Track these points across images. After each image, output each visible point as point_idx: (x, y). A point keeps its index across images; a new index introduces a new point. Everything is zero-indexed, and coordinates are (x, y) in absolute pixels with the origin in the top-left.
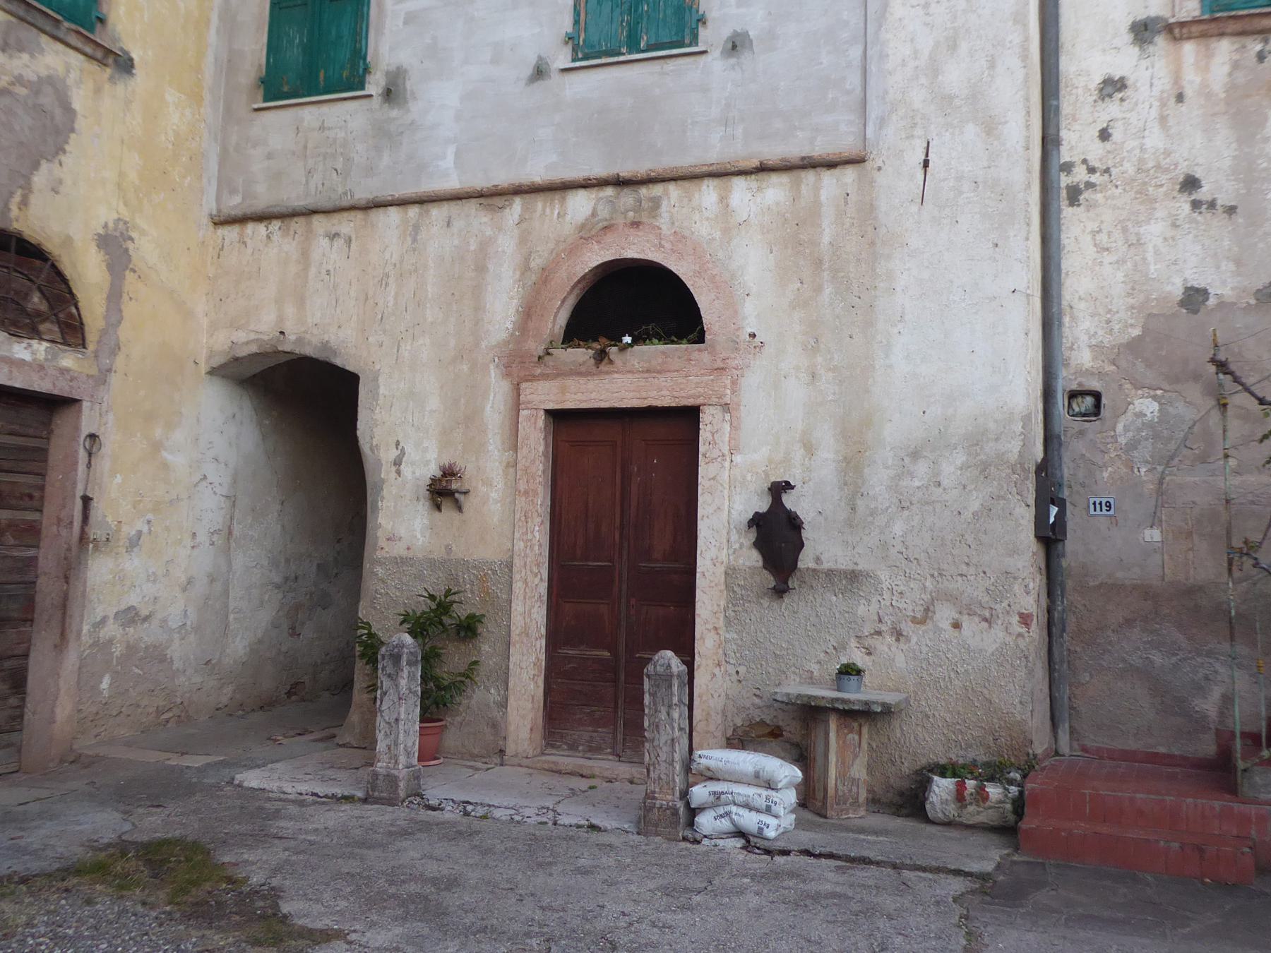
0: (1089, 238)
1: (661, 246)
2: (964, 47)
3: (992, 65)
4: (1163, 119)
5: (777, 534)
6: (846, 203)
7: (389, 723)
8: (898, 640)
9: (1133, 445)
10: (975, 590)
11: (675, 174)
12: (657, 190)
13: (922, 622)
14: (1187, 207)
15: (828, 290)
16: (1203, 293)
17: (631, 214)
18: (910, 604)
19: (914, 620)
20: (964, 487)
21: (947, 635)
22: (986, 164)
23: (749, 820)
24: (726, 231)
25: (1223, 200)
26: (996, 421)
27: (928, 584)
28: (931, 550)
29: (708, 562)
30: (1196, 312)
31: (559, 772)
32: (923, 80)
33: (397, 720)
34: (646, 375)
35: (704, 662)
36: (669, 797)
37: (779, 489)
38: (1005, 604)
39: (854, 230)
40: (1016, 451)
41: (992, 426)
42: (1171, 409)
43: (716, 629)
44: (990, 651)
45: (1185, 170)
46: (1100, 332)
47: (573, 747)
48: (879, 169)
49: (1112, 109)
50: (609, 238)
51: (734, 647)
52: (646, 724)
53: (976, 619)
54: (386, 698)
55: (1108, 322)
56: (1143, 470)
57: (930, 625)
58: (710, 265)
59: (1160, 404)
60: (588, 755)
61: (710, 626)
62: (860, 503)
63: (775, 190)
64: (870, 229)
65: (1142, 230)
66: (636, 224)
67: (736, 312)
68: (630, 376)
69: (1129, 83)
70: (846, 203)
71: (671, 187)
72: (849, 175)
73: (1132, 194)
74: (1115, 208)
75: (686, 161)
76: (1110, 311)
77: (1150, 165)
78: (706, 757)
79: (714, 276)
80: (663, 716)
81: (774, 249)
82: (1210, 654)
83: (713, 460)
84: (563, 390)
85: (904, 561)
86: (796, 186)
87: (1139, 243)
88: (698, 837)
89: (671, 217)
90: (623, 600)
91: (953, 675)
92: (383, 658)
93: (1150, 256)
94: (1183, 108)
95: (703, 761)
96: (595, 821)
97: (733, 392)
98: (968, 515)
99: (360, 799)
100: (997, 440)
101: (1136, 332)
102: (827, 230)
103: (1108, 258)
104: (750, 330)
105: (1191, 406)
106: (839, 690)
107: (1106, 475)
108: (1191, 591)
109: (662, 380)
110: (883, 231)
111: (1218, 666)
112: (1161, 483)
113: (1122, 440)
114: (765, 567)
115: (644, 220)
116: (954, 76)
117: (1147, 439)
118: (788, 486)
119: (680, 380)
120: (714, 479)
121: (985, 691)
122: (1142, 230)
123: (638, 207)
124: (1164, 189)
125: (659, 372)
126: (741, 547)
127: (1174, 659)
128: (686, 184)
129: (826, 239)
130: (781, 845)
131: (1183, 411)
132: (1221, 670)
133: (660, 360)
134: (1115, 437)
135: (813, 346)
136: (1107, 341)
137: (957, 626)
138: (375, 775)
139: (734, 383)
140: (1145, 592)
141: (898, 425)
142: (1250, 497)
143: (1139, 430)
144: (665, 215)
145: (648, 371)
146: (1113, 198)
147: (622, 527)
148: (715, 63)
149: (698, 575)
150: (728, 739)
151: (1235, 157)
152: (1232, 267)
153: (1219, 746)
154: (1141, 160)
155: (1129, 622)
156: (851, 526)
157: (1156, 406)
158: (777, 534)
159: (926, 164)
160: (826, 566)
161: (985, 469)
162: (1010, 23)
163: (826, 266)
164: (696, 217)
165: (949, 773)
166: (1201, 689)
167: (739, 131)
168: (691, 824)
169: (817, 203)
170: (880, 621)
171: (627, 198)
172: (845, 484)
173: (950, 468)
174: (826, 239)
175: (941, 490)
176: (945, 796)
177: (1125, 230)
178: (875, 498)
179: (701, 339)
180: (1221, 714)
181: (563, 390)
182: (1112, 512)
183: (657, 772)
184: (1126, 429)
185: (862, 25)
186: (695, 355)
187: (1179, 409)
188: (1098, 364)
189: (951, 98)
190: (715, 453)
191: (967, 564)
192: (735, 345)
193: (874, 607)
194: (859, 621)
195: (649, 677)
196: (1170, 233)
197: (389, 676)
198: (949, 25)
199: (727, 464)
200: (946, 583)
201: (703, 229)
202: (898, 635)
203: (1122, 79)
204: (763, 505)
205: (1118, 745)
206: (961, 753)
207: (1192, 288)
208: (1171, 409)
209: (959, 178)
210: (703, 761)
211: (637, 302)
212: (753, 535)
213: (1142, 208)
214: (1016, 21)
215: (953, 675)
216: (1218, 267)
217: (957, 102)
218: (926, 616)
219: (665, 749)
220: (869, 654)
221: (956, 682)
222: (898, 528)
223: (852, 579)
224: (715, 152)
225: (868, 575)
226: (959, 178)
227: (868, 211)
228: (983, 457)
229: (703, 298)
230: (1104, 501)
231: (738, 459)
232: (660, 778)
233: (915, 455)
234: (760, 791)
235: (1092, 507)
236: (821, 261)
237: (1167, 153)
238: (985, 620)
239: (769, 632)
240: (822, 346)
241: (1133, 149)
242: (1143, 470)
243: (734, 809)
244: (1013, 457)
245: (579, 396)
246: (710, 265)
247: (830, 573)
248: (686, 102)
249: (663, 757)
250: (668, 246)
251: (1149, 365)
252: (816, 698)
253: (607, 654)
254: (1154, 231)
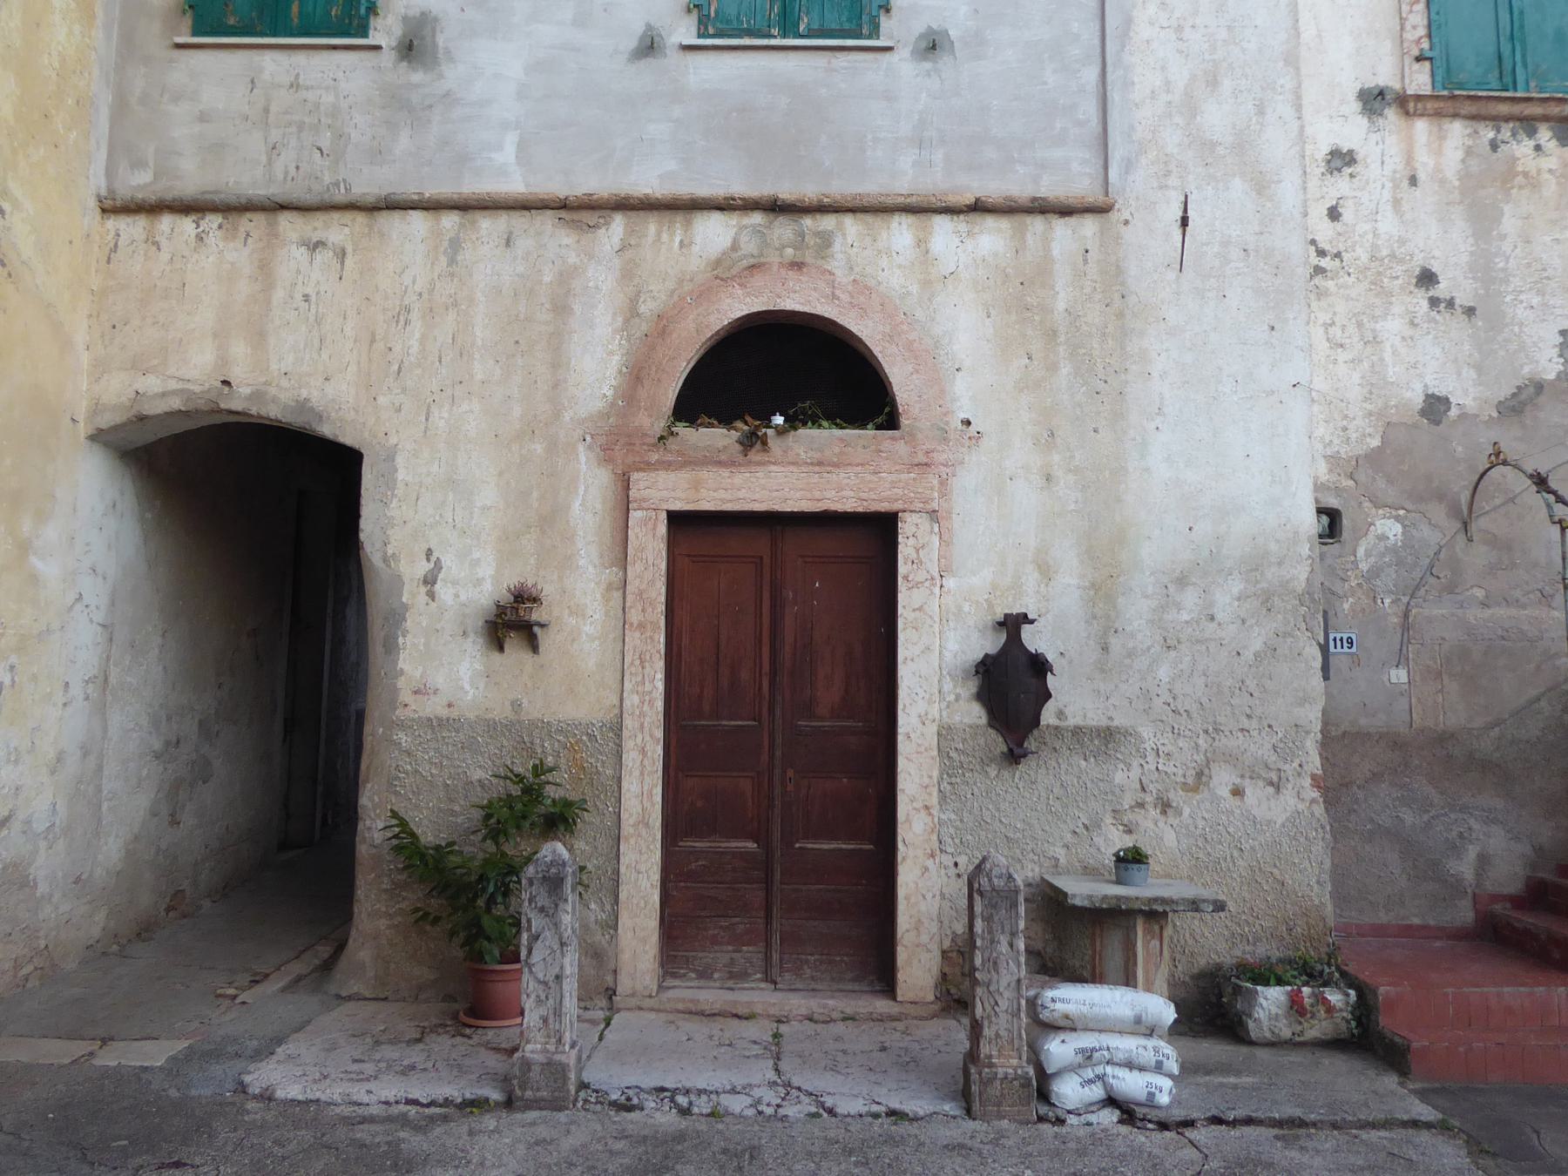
0: (1321, 330)
1: (834, 296)
2: (1227, 84)
3: (1261, 111)
4: (1396, 203)
5: (1011, 684)
6: (1086, 261)
7: (545, 983)
8: (1164, 812)
9: (1375, 572)
10: (1260, 748)
11: (857, 203)
12: (828, 222)
13: (1195, 789)
14: (1425, 304)
15: (1065, 369)
16: (1445, 401)
17: (790, 251)
18: (1179, 767)
19: (1185, 787)
20: (1244, 621)
21: (1226, 806)
22: (1257, 229)
23: (1131, 1084)
24: (926, 283)
25: (1462, 299)
26: (1278, 541)
27: (1201, 742)
28: (1204, 700)
29: (915, 721)
30: (1438, 423)
31: (702, 1014)
32: (1178, 119)
33: (558, 978)
34: (817, 469)
35: (911, 853)
36: (1015, 1062)
37: (1013, 624)
38: (1295, 765)
39: (1098, 297)
40: (1304, 576)
41: (1273, 547)
42: (1414, 532)
43: (927, 807)
44: (1279, 822)
45: (1421, 262)
46: (1336, 441)
47: (705, 974)
48: (1126, 222)
49: (1340, 186)
50: (758, 280)
51: (952, 831)
52: (978, 961)
53: (1261, 783)
54: (538, 945)
55: (1345, 429)
56: (1387, 601)
57: (1204, 794)
58: (905, 327)
59: (1404, 527)
60: (730, 984)
61: (918, 805)
62: (1115, 642)
63: (992, 236)
64: (1117, 296)
65: (1378, 326)
66: (797, 266)
67: (943, 391)
68: (792, 468)
69: (1359, 157)
70: (1086, 261)
71: (848, 220)
72: (1088, 226)
73: (1365, 285)
74: (1348, 298)
75: (869, 188)
76: (1346, 417)
77: (1385, 252)
78: (1063, 1001)
79: (912, 342)
80: (1004, 948)
81: (993, 312)
82: (1464, 809)
83: (918, 585)
84: (696, 485)
85: (1171, 714)
86: (1020, 234)
87: (1375, 341)
88: (1060, 1113)
89: (849, 260)
90: (777, 771)
91: (1236, 854)
92: (531, 882)
93: (1388, 356)
94: (1418, 192)
95: (1058, 1006)
96: (895, 1105)
97: (943, 495)
98: (1248, 655)
99: (497, 1104)
100: (1280, 564)
101: (1375, 442)
102: (1062, 295)
103: (1342, 356)
104: (963, 416)
105: (1435, 530)
106: (1119, 882)
107: (1346, 606)
108: (1443, 739)
109: (839, 477)
110: (1132, 300)
111: (1472, 822)
112: (1406, 615)
113: (1364, 566)
114: (991, 725)
115: (809, 260)
116: (1217, 118)
117: (1390, 566)
118: (1024, 619)
119: (869, 477)
120: (920, 609)
121: (1276, 871)
122: (1378, 326)
123: (800, 241)
124: (1400, 281)
125: (836, 465)
126: (957, 700)
127: (1426, 817)
128: (869, 218)
129: (1061, 305)
130: (1178, 1114)
131: (1429, 536)
132: (1476, 826)
133: (837, 450)
134: (1355, 563)
135: (1049, 439)
136: (1344, 451)
137: (1237, 792)
138: (527, 1065)
139: (943, 483)
140: (1396, 743)
141: (1157, 547)
142: (1500, 632)
143: (1383, 555)
144: (839, 256)
145: (820, 464)
146: (1346, 287)
147: (773, 673)
148: (902, 64)
149: (900, 738)
150: (943, 952)
151: (1472, 253)
152: (1473, 374)
153: (1477, 911)
154: (1374, 247)
155: (1376, 777)
156: (1103, 671)
157: (1398, 528)
158: (1011, 684)
159: (1184, 222)
160: (1071, 722)
161: (1267, 601)
162: (1281, 64)
163: (1062, 339)
164: (884, 262)
165: (1272, 981)
166: (1455, 849)
167: (939, 156)
168: (1044, 1095)
169: (1047, 257)
170: (1143, 789)
171: (783, 229)
172: (1095, 617)
173: (1227, 597)
174: (1061, 305)
175: (1213, 625)
176: (1274, 1010)
177: (1360, 325)
178: (1132, 636)
179: (891, 422)
180: (1478, 875)
181: (696, 485)
182: (1354, 649)
183: (994, 1028)
184: (1368, 554)
185: (1097, 42)
186: (887, 445)
187: (1425, 532)
188: (1334, 478)
189: (1213, 145)
190: (921, 576)
191: (1249, 717)
192: (943, 435)
193: (1135, 773)
194: (1117, 791)
195: (981, 894)
196: (1408, 332)
197: (542, 909)
198: (1207, 57)
199: (937, 590)
200: (1224, 740)
201: (894, 278)
202: (1165, 806)
203: (1351, 152)
204: (992, 644)
205: (1367, 919)
206: (1248, 948)
207: (1433, 396)
208: (1414, 532)
209: (1226, 244)
210: (1058, 1006)
211: (793, 370)
212: (973, 686)
213: (1378, 301)
214: (1287, 62)
215: (1236, 854)
216: (1459, 374)
217: (1220, 150)
218: (1199, 780)
219: (1007, 994)
220: (1129, 832)
221: (1240, 862)
222: (1164, 673)
223: (1105, 740)
224: (904, 180)
225: (1126, 733)
226: (1226, 244)
227: (1114, 275)
228: (1264, 585)
229: (895, 370)
230: (1345, 637)
231: (950, 583)
232: (997, 1035)
233: (1182, 581)
234: (1143, 1041)
235: (1332, 643)
236: (1055, 332)
237: (1402, 242)
238: (1271, 784)
239: (998, 810)
240: (1059, 441)
241: (1365, 233)
242: (1387, 601)
243: (1109, 1069)
244: (1300, 585)
245: (722, 494)
246: (905, 327)
247: (1077, 731)
248: (862, 110)
249: (1004, 1004)
250: (845, 297)
251: (1390, 481)
252: (1127, 899)
253: (751, 845)
254: (1392, 327)
